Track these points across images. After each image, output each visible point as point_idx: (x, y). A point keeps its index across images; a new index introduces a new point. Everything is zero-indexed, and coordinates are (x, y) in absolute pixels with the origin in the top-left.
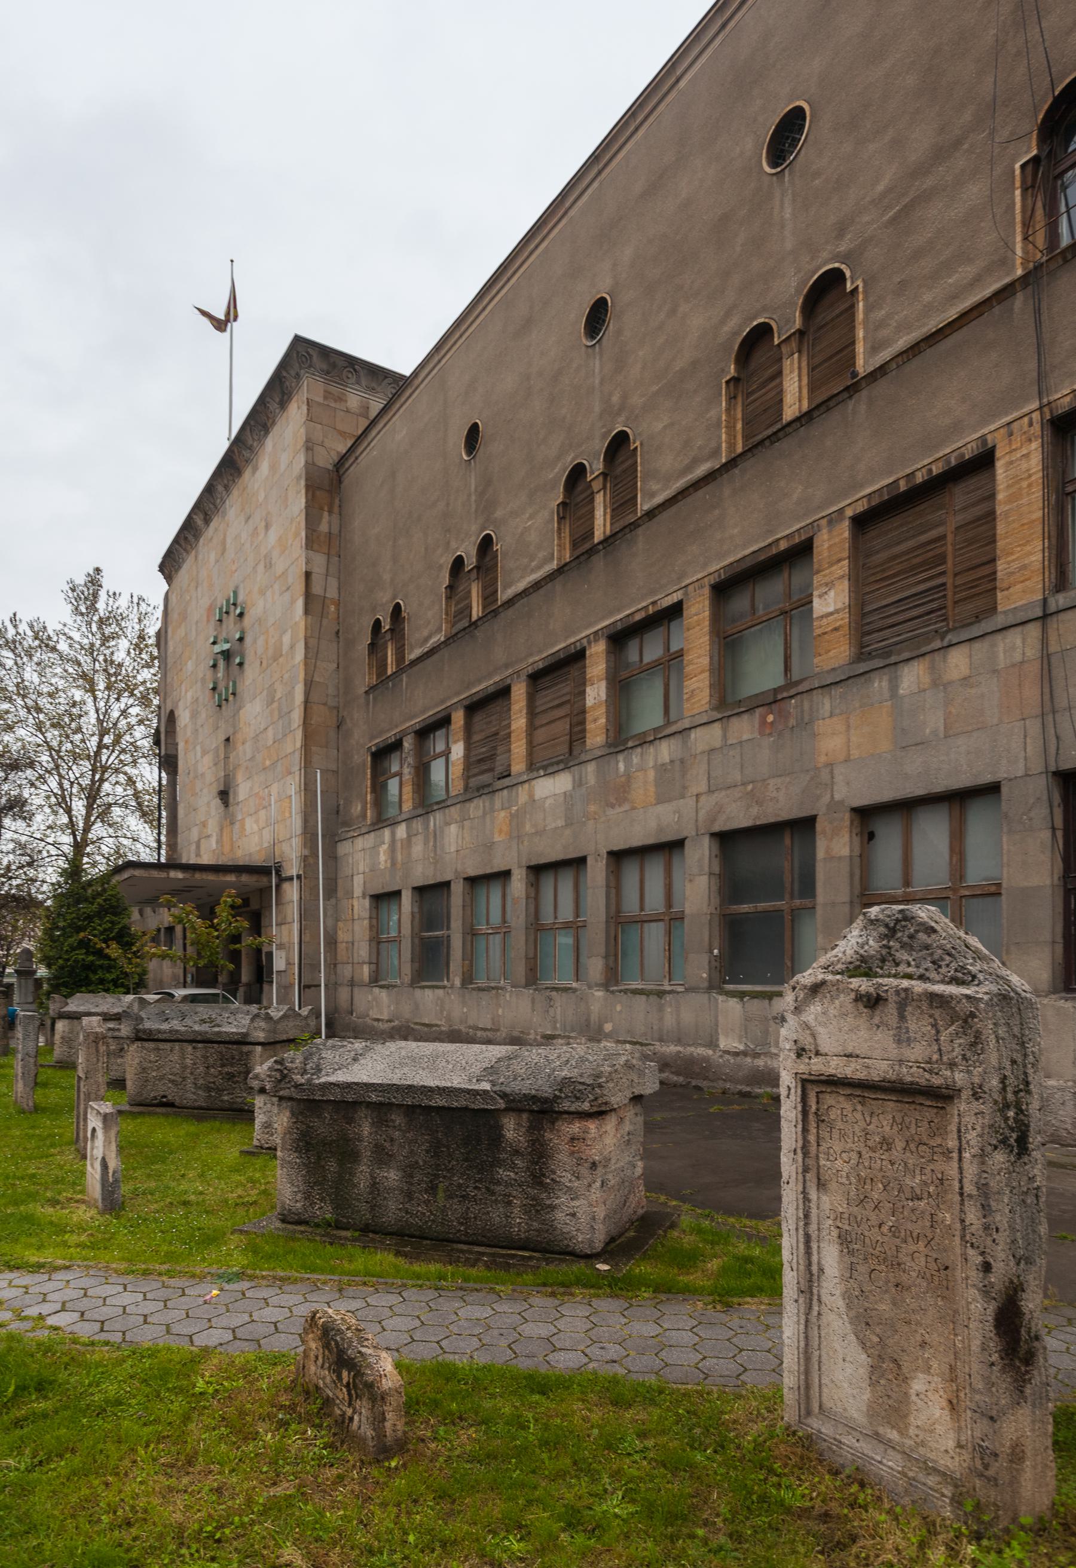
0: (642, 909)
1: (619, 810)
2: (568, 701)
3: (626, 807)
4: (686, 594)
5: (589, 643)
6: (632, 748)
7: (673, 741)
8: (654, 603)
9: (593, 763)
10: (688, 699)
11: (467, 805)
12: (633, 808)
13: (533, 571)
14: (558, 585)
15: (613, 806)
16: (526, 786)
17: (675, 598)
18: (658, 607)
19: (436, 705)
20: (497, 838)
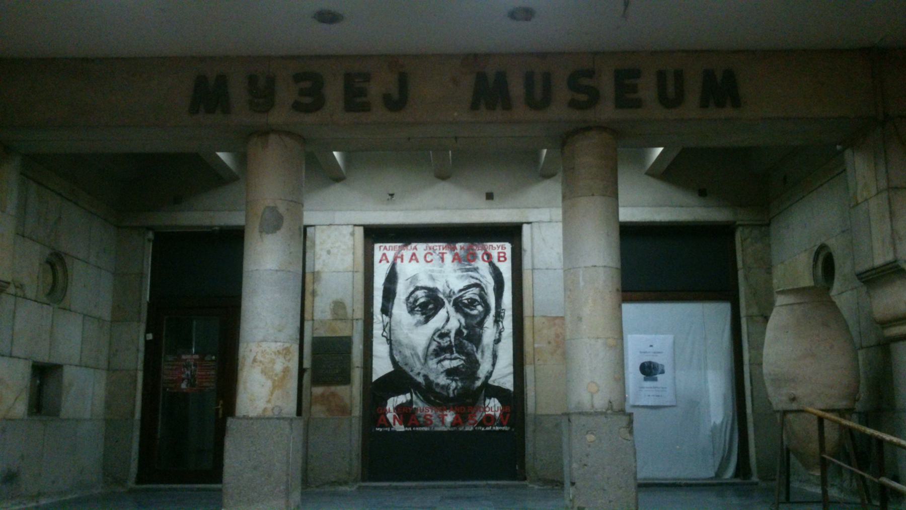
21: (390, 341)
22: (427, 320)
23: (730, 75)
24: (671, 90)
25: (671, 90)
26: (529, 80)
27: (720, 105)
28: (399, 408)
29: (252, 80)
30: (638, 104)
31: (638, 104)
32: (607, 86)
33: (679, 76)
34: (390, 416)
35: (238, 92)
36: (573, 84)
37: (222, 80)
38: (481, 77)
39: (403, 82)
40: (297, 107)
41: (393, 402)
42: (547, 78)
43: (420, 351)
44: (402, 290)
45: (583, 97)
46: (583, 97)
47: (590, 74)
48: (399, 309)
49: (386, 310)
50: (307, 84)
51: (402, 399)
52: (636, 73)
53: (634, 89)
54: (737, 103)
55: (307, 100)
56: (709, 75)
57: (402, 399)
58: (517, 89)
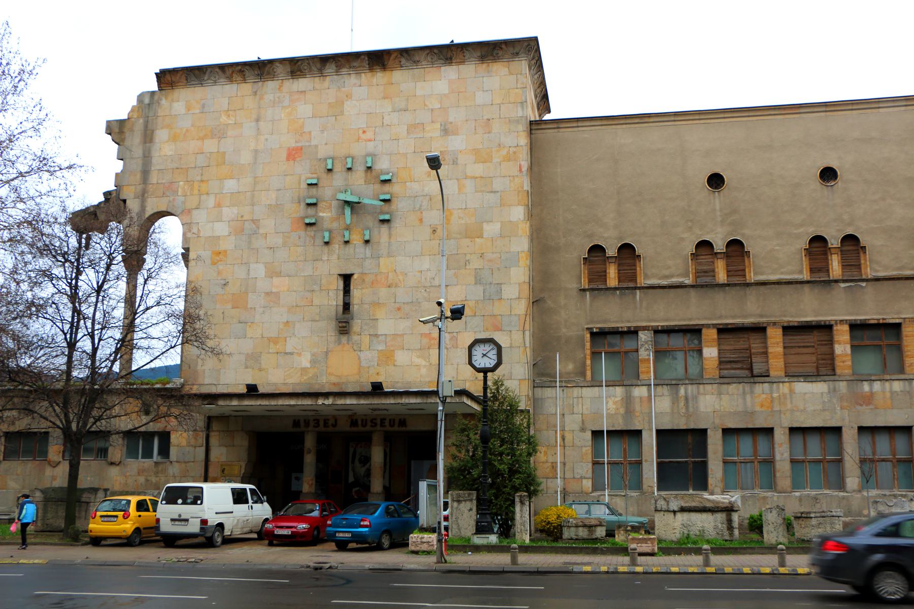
0: (874, 453)
1: (864, 407)
2: (813, 347)
3: (871, 407)
4: (905, 321)
5: (836, 324)
6: (874, 380)
7: (901, 382)
8: (883, 319)
9: (845, 382)
10: (909, 366)
11: (725, 386)
12: (876, 408)
13: (782, 273)
14: (806, 288)
15: (861, 405)
16: (787, 384)
17: (897, 321)
18: (885, 322)
19: (679, 320)
20: (758, 409)
21: (353, 471)
22: (364, 466)
23: (405, 420)
24: (392, 423)
25: (392, 423)
26: (362, 420)
27: (402, 427)
28: (356, 492)
29: (305, 421)
30: (385, 426)
31: (385, 426)
32: (379, 422)
33: (394, 420)
34: (353, 494)
35: (302, 424)
36: (372, 421)
37: (299, 421)
38: (352, 420)
39: (336, 420)
40: (314, 426)
41: (354, 490)
42: (366, 420)
43: (362, 475)
44: (357, 457)
45: (373, 425)
46: (373, 425)
47: (375, 419)
48: (357, 462)
49: (353, 462)
50: (316, 422)
51: (357, 489)
52: (385, 419)
53: (384, 423)
54: (406, 426)
55: (316, 425)
56: (400, 420)
57: (357, 489)
58: (360, 423)
